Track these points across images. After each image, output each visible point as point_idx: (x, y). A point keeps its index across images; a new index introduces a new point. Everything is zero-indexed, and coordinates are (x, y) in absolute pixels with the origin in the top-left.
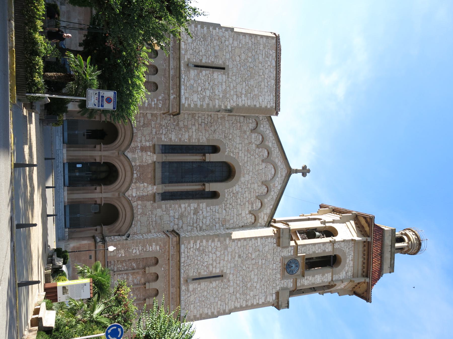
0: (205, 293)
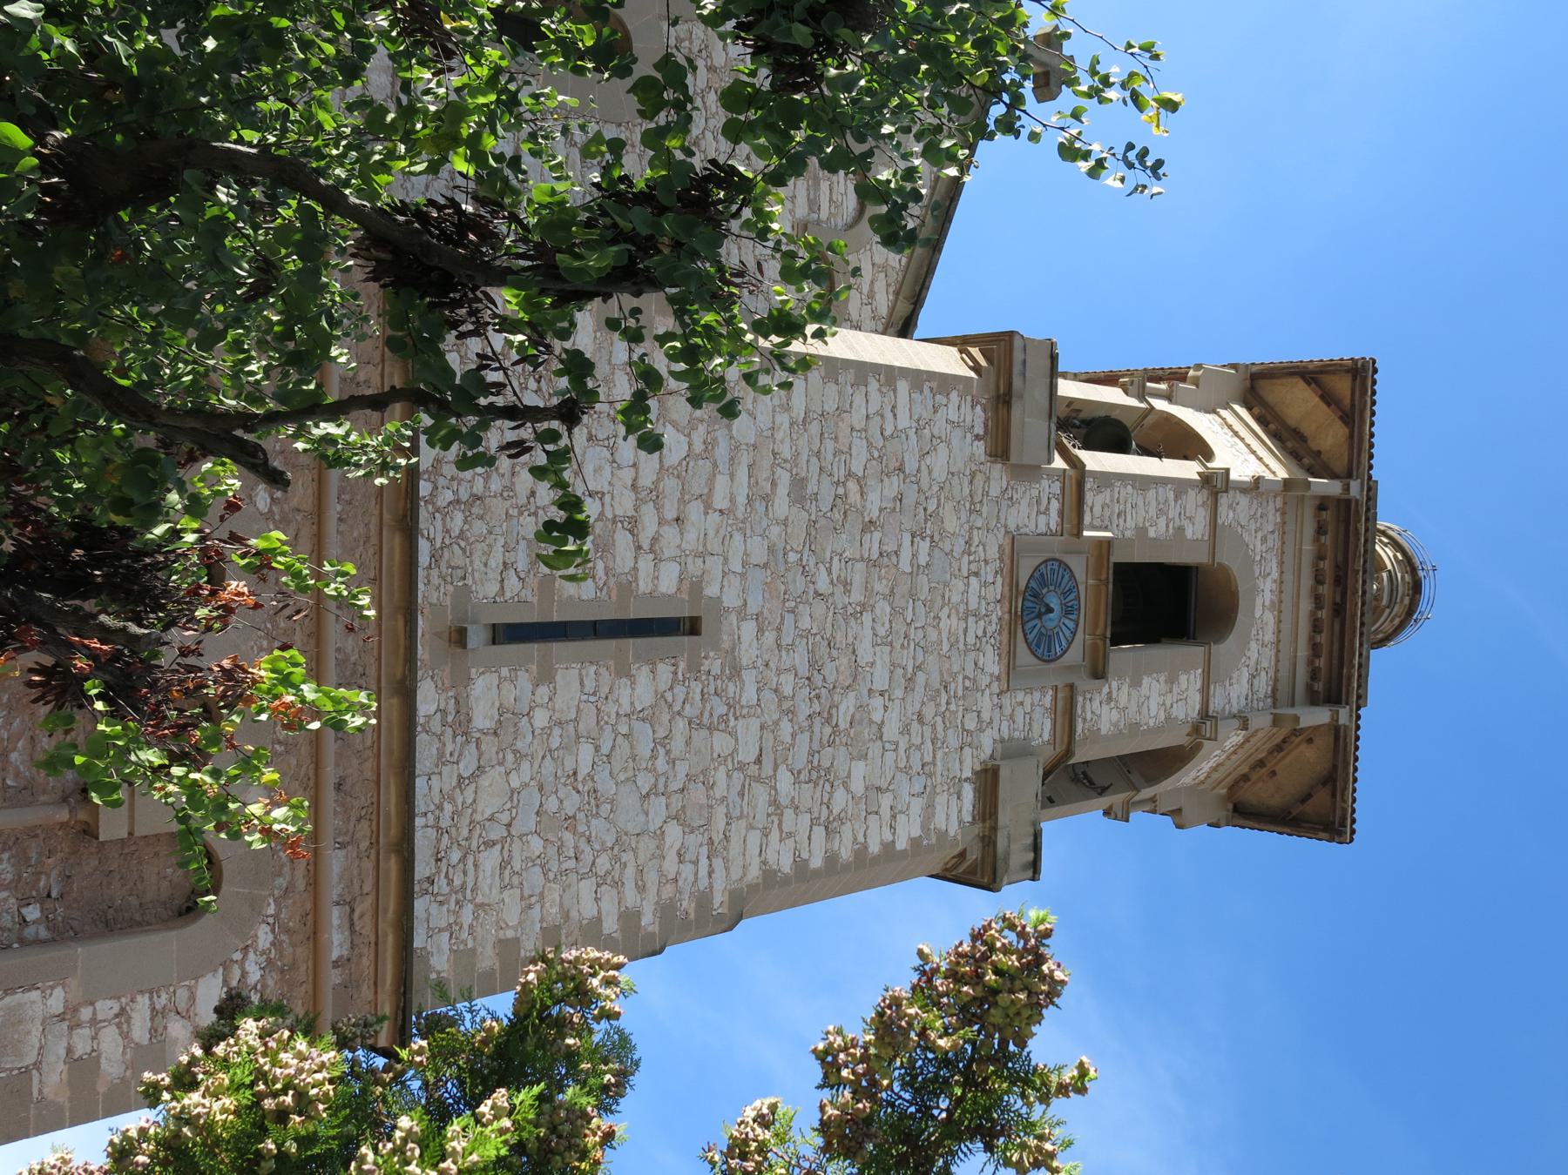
0: (586, 752)
